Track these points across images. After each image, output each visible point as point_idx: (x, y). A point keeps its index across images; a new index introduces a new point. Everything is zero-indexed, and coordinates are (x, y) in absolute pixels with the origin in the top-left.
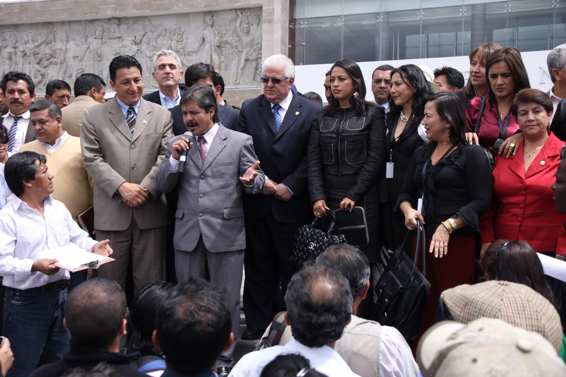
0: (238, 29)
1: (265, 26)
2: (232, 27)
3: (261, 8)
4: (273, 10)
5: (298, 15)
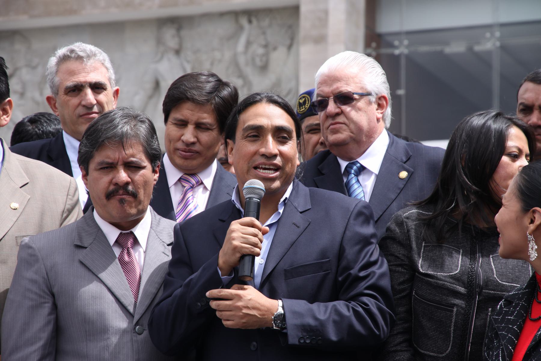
0: (242, 60)
1: (305, 51)
2: (228, 55)
3: (295, 10)
4: (326, 12)
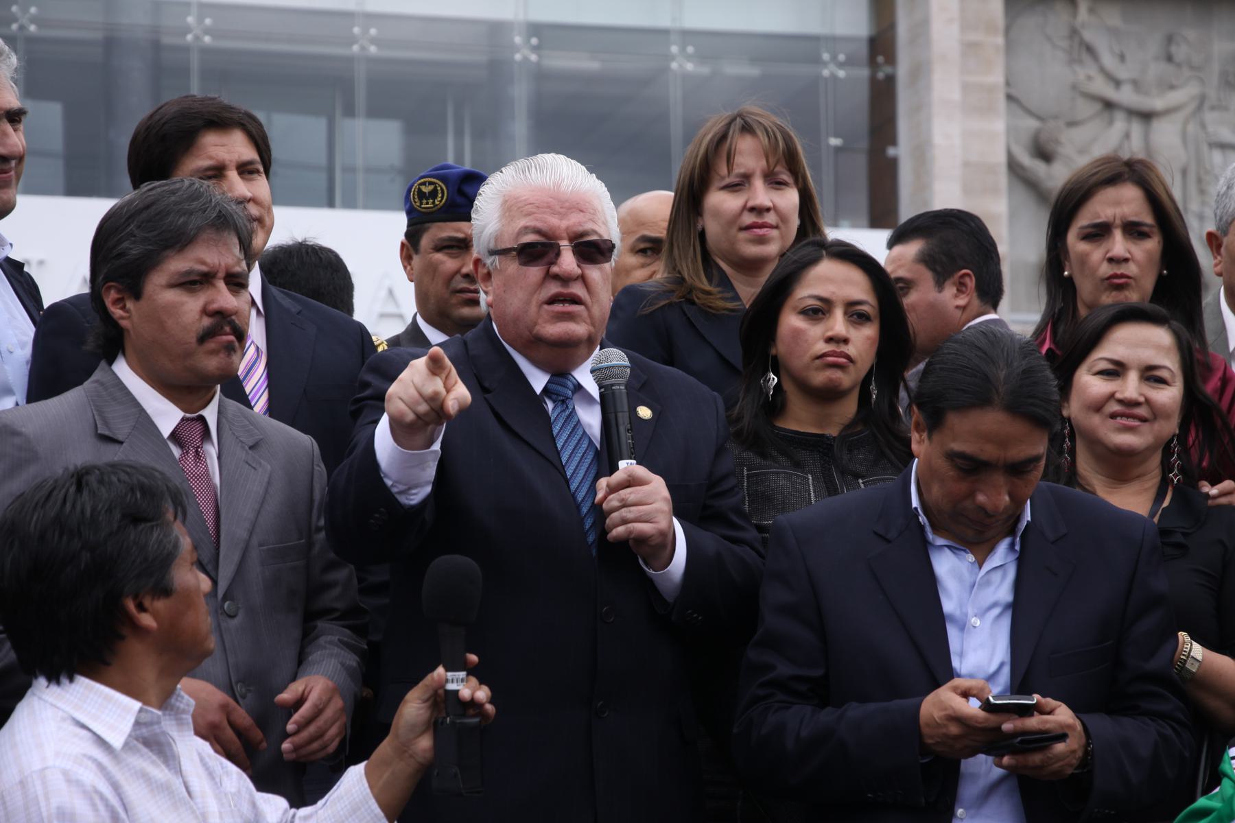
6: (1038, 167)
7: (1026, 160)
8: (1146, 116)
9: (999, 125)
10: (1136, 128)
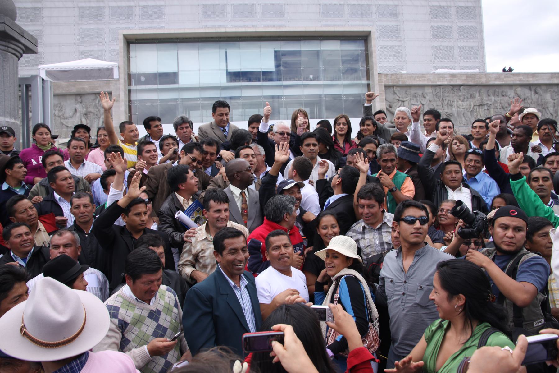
0: (97, 105)
2: (94, 104)
3: (110, 93)
4: (119, 95)
5: (134, 97)
6: (390, 109)
7: (388, 108)
8: (404, 101)
9: (385, 104)
10: (402, 103)
